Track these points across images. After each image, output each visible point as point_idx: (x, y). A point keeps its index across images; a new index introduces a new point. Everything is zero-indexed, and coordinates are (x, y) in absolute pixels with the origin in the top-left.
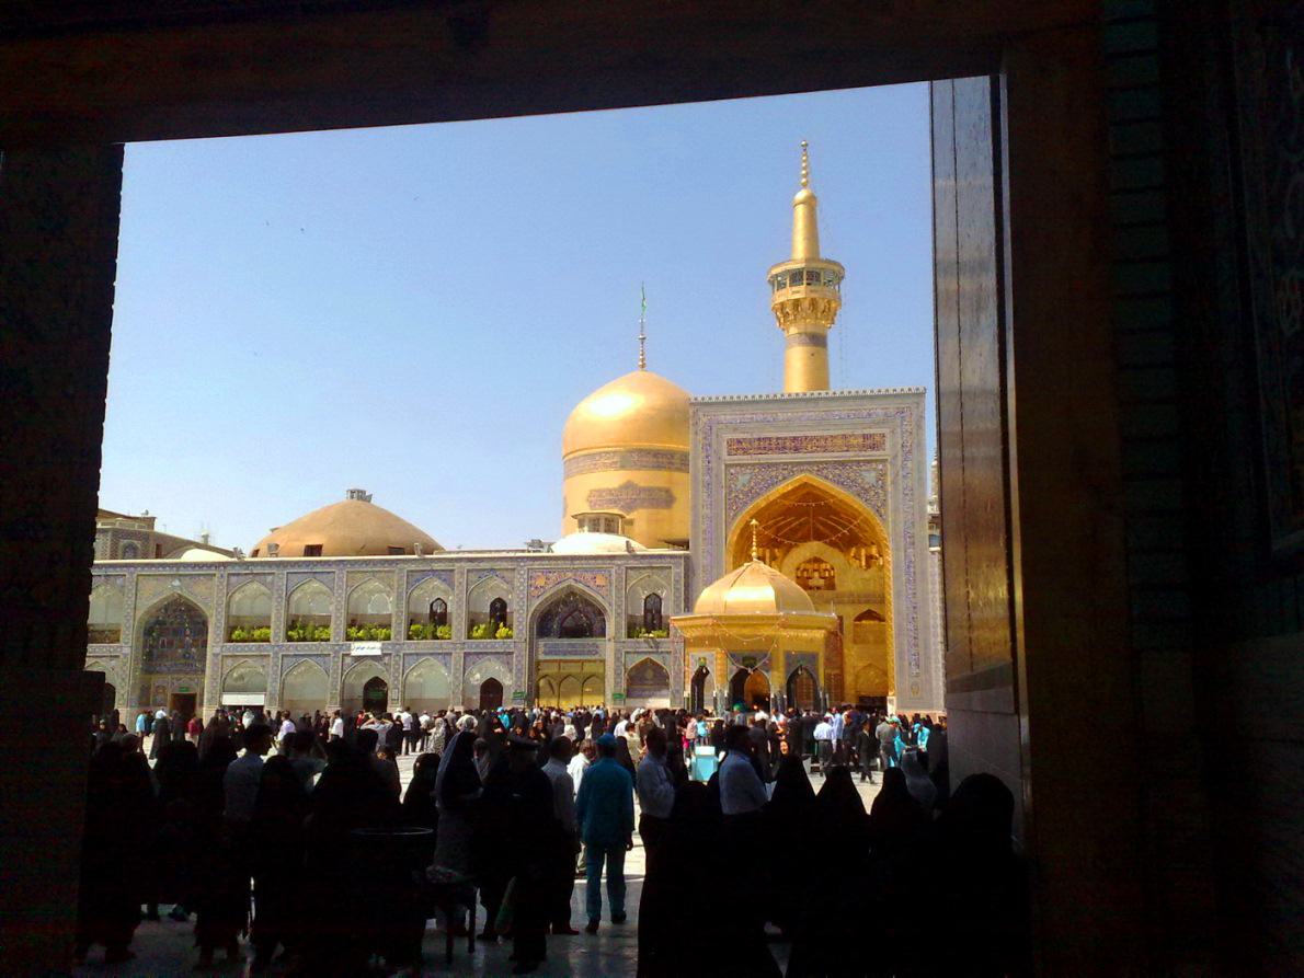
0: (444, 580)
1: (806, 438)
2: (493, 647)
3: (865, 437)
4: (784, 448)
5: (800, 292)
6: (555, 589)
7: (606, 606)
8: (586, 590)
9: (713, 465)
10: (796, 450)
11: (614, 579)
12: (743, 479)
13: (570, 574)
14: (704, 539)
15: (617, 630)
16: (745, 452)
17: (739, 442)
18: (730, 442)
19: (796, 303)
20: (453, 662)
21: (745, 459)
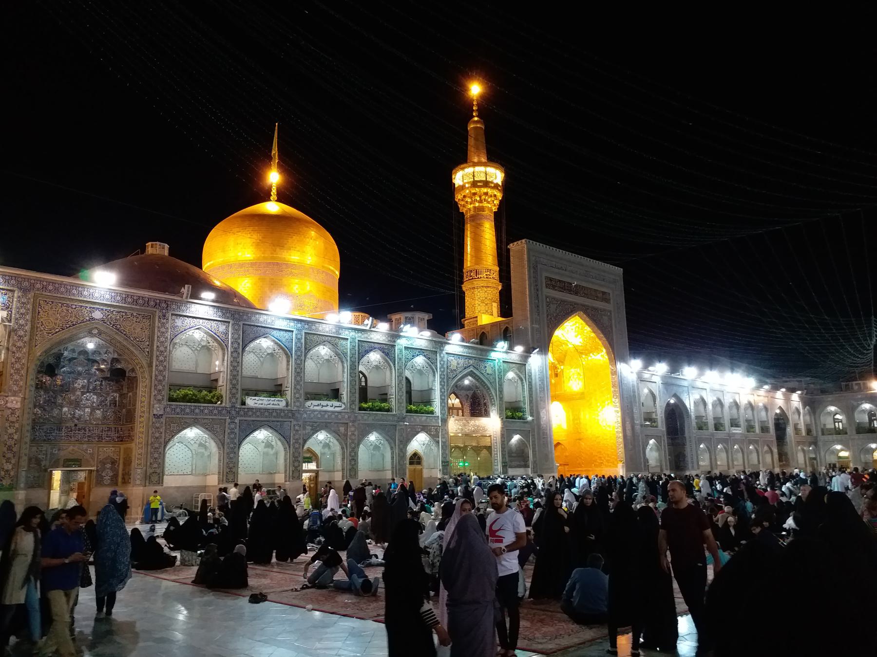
3: (604, 293)
10: (576, 293)
16: (554, 287)
17: (551, 279)
18: (547, 278)
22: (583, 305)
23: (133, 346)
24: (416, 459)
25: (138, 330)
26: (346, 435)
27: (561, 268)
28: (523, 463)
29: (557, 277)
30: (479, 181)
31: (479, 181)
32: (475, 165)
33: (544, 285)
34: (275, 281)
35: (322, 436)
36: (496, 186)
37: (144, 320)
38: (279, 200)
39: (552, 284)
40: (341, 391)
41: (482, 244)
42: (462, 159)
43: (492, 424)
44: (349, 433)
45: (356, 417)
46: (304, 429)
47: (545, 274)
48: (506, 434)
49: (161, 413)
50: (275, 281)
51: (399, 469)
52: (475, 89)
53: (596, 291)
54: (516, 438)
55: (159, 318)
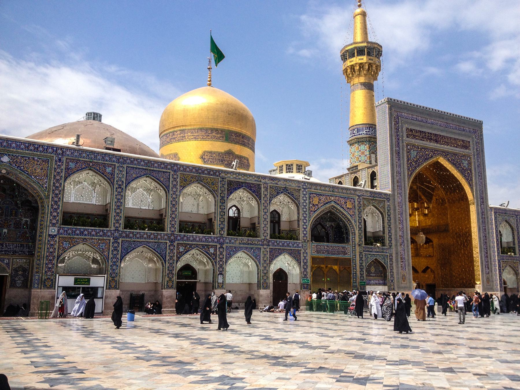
0: (254, 192)
1: (440, 136)
2: (288, 245)
4: (431, 139)
5: (364, 59)
6: (323, 208)
7: (353, 222)
8: (342, 210)
9: (401, 142)
10: (437, 141)
11: (357, 203)
12: (414, 153)
13: (333, 198)
14: (398, 186)
15: (360, 239)
16: (414, 137)
17: (411, 130)
18: (407, 129)
19: (361, 65)
20: (262, 256)
21: (413, 141)
22: (444, 152)
23: (34, 182)
25: (38, 170)
26: (215, 254)
27: (422, 121)
28: (381, 282)
29: (418, 129)
33: (405, 136)
37: (44, 163)
39: (411, 133)
40: (213, 220)
44: (218, 253)
45: (224, 241)
46: (178, 249)
47: (406, 126)
49: (55, 233)
53: (455, 139)
55: (56, 161)
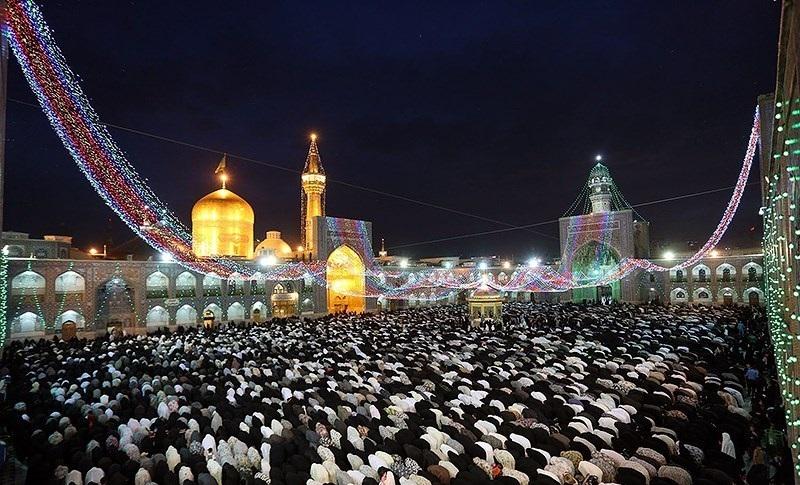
24: (257, 311)
30: (313, 180)
31: (313, 180)
32: (311, 173)
34: (221, 225)
35: (213, 305)
36: (320, 183)
38: (226, 188)
41: (314, 210)
42: (307, 171)
43: (294, 296)
48: (301, 299)
50: (221, 225)
51: (247, 317)
52: (314, 137)
54: (307, 301)
